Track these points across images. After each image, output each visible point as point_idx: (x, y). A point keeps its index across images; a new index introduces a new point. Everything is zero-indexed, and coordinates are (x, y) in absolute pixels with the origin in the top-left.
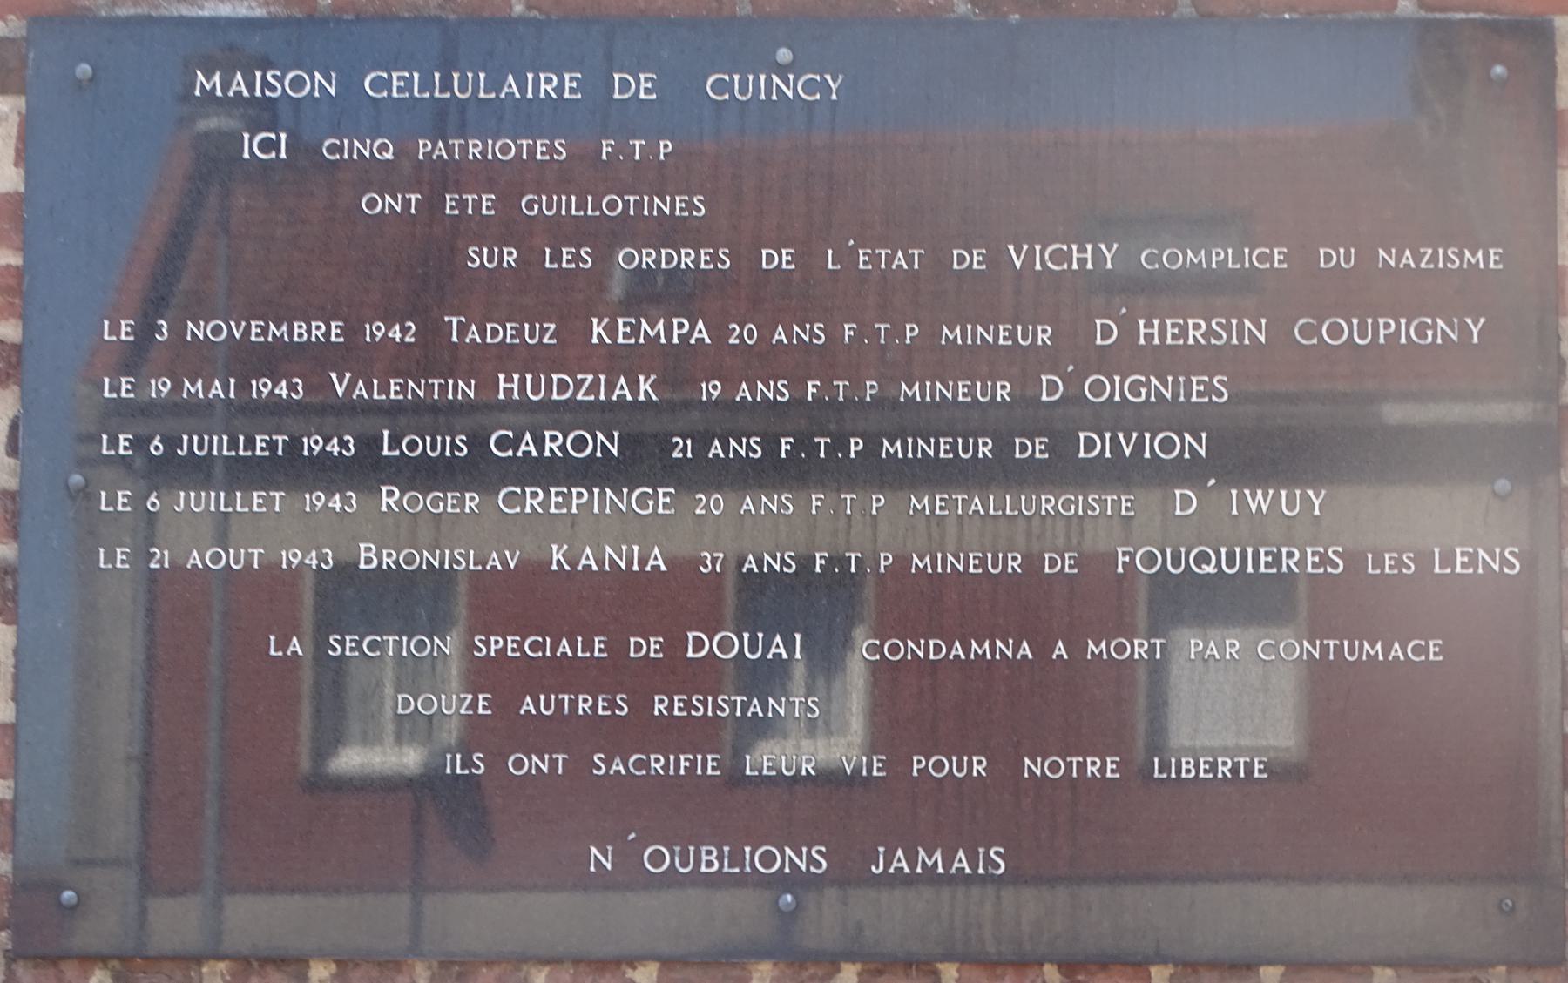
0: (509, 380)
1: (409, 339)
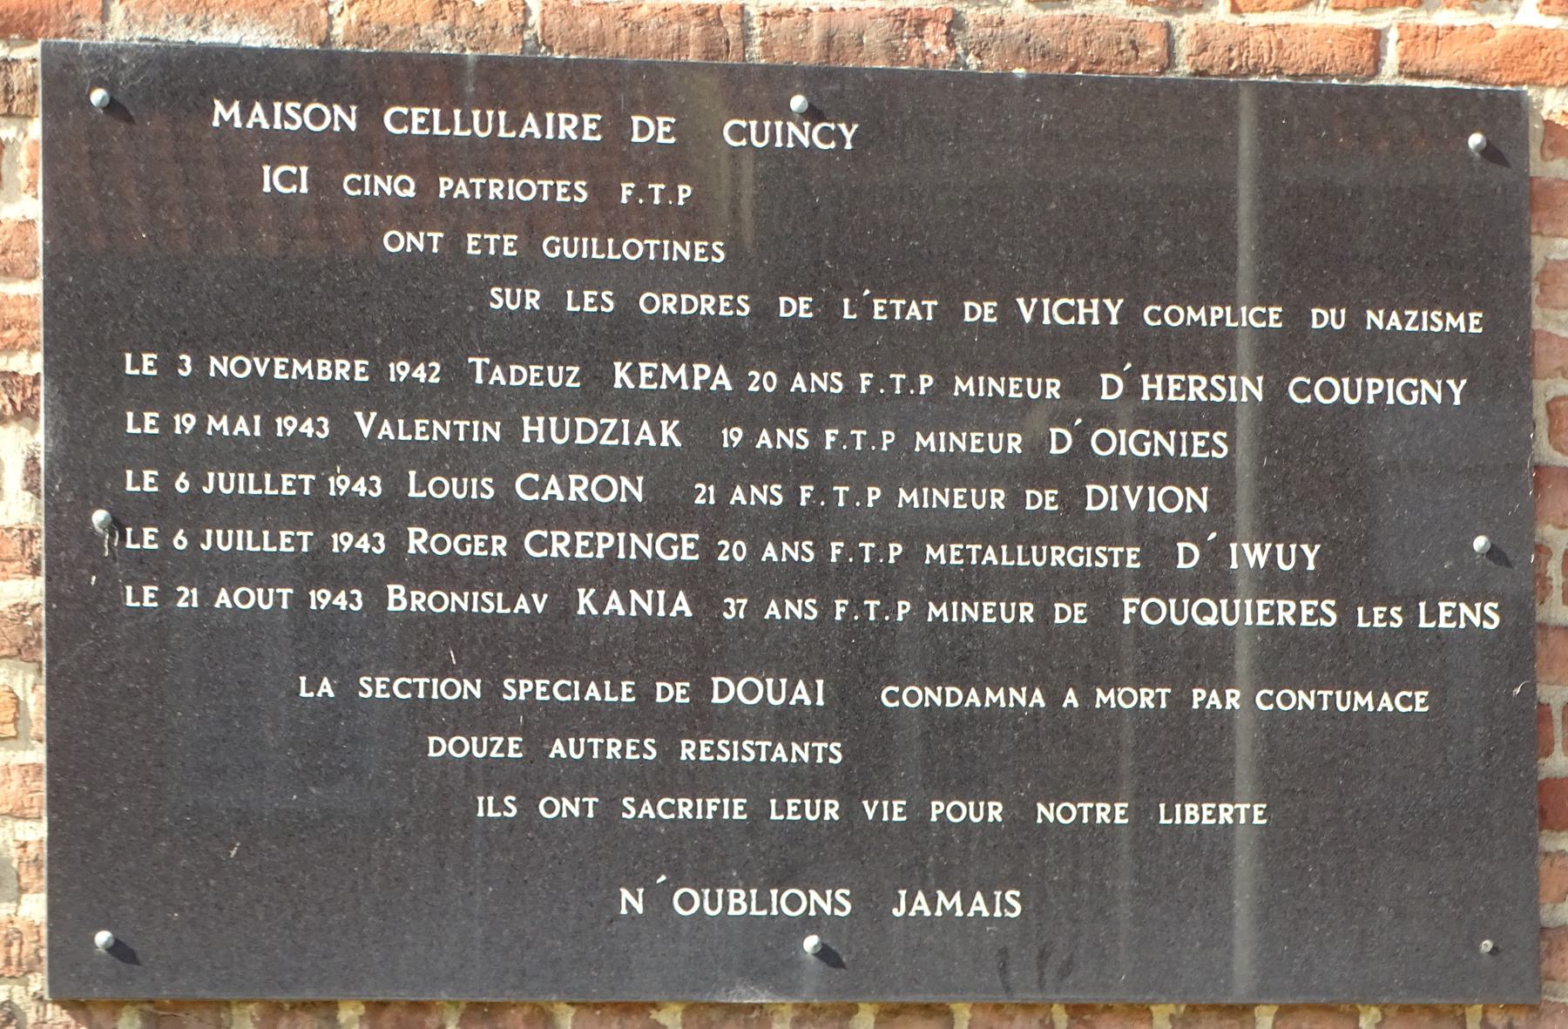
0: (534, 423)
1: (434, 380)
